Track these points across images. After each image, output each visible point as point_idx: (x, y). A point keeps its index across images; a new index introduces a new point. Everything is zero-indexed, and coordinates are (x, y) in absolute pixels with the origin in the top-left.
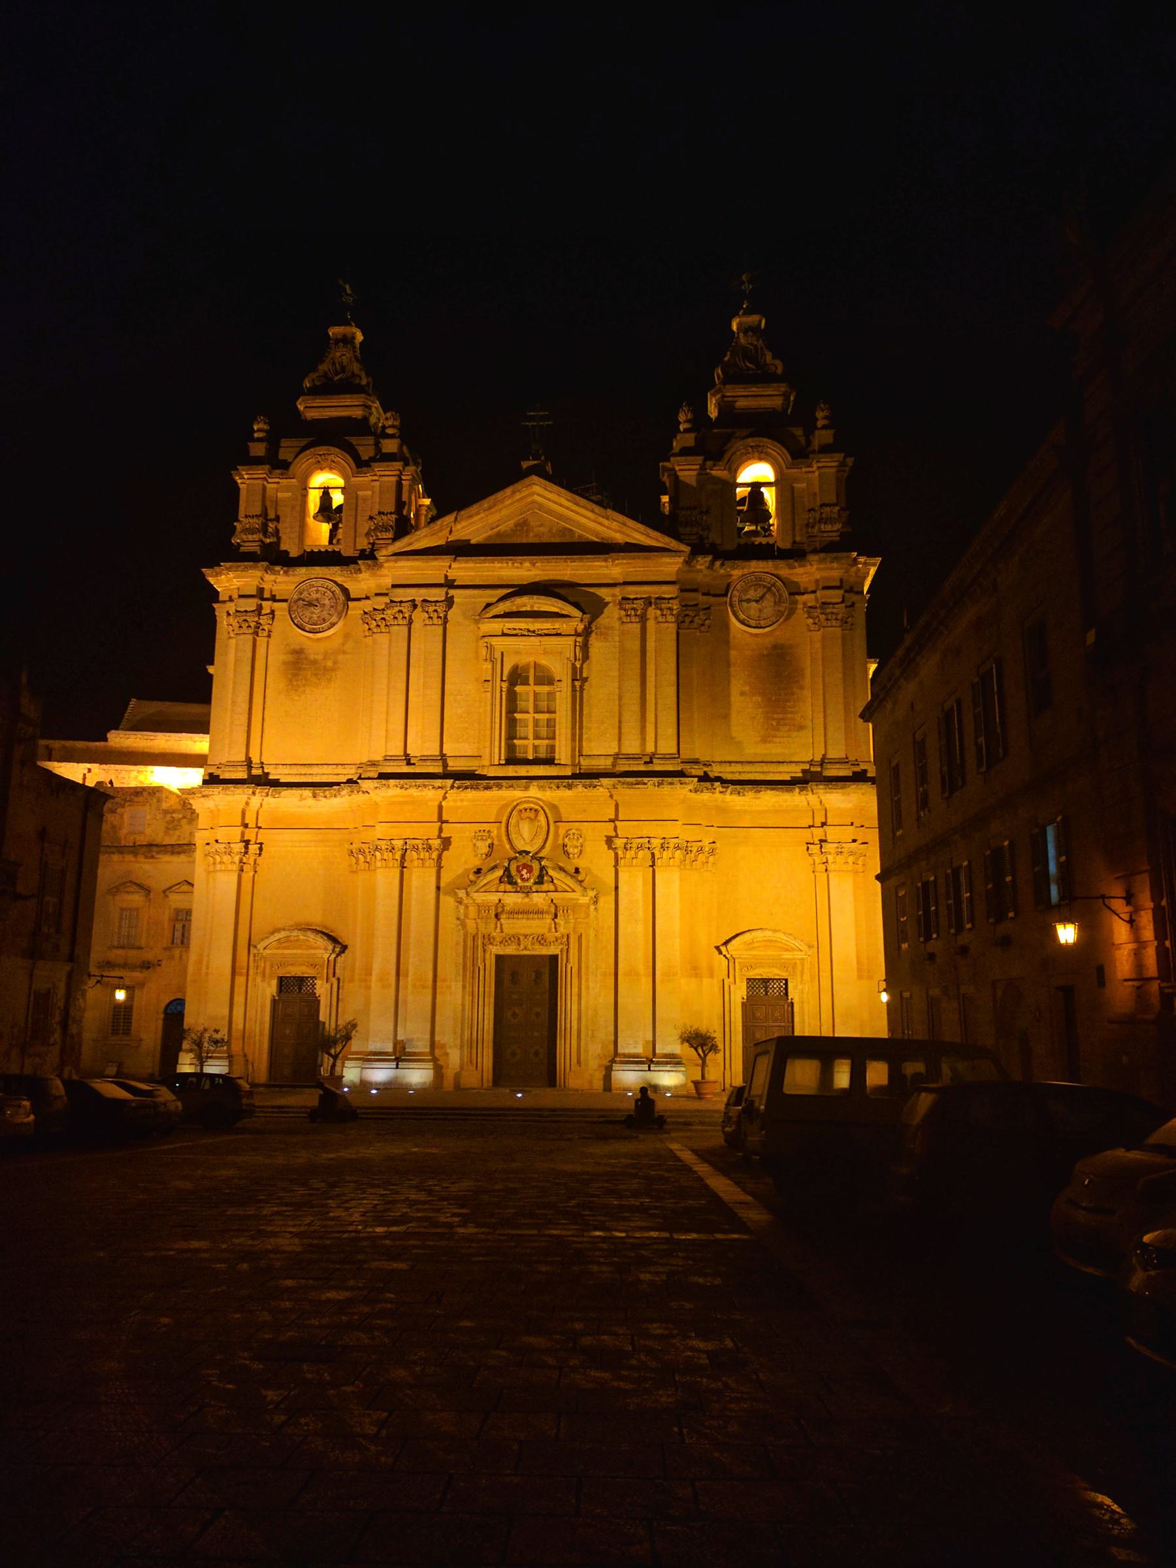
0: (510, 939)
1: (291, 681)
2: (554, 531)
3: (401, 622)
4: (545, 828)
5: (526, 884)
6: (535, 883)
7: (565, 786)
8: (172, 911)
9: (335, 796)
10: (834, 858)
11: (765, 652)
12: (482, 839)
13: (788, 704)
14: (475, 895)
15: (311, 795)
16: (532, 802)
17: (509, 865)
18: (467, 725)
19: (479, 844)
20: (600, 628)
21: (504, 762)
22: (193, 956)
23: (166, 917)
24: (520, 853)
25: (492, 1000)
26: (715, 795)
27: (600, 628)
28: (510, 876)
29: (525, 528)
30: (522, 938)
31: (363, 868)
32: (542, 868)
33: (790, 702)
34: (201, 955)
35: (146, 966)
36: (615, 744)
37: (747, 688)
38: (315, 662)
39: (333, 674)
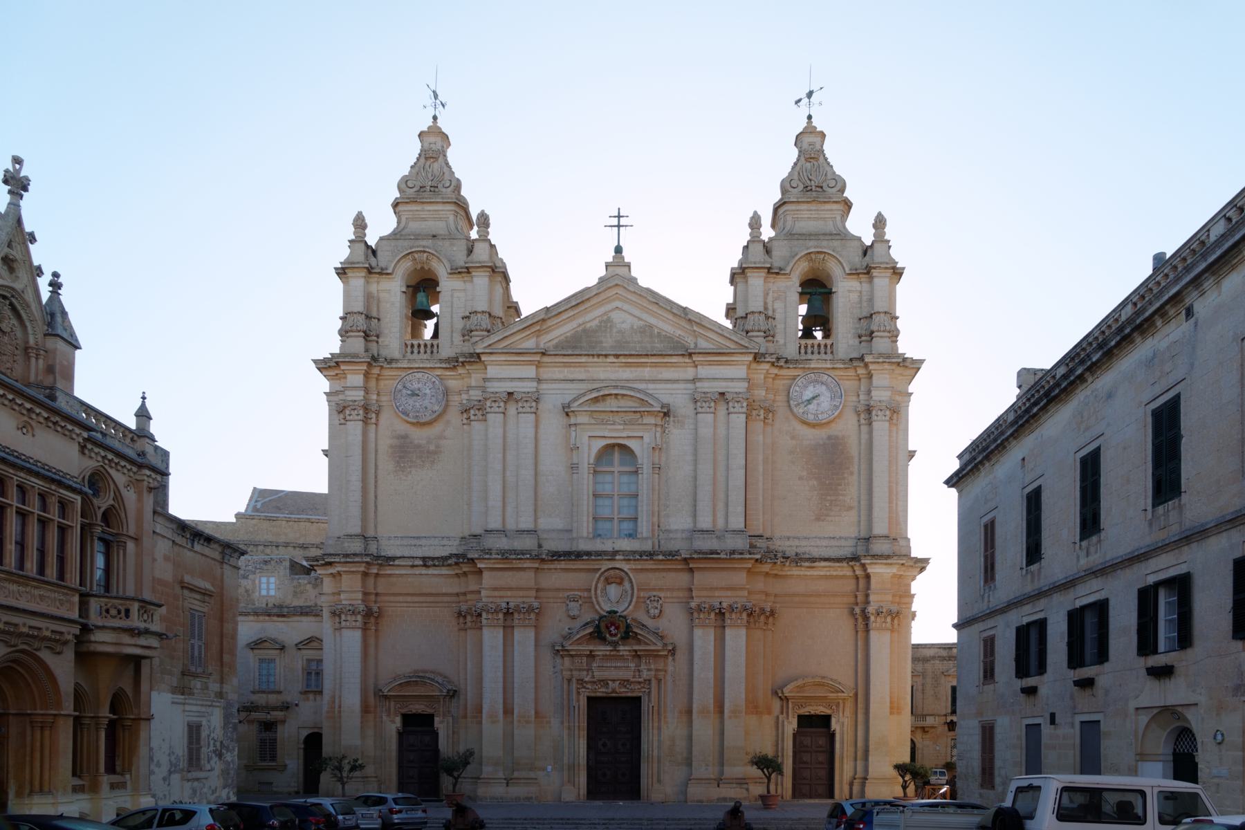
1: (398, 462)
4: (630, 592)
5: (614, 639)
6: (622, 638)
8: (305, 661)
12: (574, 601)
15: (421, 563)
19: (572, 604)
21: (591, 536)
23: (300, 667)
24: (609, 612)
25: (586, 732)
30: (609, 682)
35: (286, 707)
36: (689, 520)
38: (419, 446)
39: (436, 457)
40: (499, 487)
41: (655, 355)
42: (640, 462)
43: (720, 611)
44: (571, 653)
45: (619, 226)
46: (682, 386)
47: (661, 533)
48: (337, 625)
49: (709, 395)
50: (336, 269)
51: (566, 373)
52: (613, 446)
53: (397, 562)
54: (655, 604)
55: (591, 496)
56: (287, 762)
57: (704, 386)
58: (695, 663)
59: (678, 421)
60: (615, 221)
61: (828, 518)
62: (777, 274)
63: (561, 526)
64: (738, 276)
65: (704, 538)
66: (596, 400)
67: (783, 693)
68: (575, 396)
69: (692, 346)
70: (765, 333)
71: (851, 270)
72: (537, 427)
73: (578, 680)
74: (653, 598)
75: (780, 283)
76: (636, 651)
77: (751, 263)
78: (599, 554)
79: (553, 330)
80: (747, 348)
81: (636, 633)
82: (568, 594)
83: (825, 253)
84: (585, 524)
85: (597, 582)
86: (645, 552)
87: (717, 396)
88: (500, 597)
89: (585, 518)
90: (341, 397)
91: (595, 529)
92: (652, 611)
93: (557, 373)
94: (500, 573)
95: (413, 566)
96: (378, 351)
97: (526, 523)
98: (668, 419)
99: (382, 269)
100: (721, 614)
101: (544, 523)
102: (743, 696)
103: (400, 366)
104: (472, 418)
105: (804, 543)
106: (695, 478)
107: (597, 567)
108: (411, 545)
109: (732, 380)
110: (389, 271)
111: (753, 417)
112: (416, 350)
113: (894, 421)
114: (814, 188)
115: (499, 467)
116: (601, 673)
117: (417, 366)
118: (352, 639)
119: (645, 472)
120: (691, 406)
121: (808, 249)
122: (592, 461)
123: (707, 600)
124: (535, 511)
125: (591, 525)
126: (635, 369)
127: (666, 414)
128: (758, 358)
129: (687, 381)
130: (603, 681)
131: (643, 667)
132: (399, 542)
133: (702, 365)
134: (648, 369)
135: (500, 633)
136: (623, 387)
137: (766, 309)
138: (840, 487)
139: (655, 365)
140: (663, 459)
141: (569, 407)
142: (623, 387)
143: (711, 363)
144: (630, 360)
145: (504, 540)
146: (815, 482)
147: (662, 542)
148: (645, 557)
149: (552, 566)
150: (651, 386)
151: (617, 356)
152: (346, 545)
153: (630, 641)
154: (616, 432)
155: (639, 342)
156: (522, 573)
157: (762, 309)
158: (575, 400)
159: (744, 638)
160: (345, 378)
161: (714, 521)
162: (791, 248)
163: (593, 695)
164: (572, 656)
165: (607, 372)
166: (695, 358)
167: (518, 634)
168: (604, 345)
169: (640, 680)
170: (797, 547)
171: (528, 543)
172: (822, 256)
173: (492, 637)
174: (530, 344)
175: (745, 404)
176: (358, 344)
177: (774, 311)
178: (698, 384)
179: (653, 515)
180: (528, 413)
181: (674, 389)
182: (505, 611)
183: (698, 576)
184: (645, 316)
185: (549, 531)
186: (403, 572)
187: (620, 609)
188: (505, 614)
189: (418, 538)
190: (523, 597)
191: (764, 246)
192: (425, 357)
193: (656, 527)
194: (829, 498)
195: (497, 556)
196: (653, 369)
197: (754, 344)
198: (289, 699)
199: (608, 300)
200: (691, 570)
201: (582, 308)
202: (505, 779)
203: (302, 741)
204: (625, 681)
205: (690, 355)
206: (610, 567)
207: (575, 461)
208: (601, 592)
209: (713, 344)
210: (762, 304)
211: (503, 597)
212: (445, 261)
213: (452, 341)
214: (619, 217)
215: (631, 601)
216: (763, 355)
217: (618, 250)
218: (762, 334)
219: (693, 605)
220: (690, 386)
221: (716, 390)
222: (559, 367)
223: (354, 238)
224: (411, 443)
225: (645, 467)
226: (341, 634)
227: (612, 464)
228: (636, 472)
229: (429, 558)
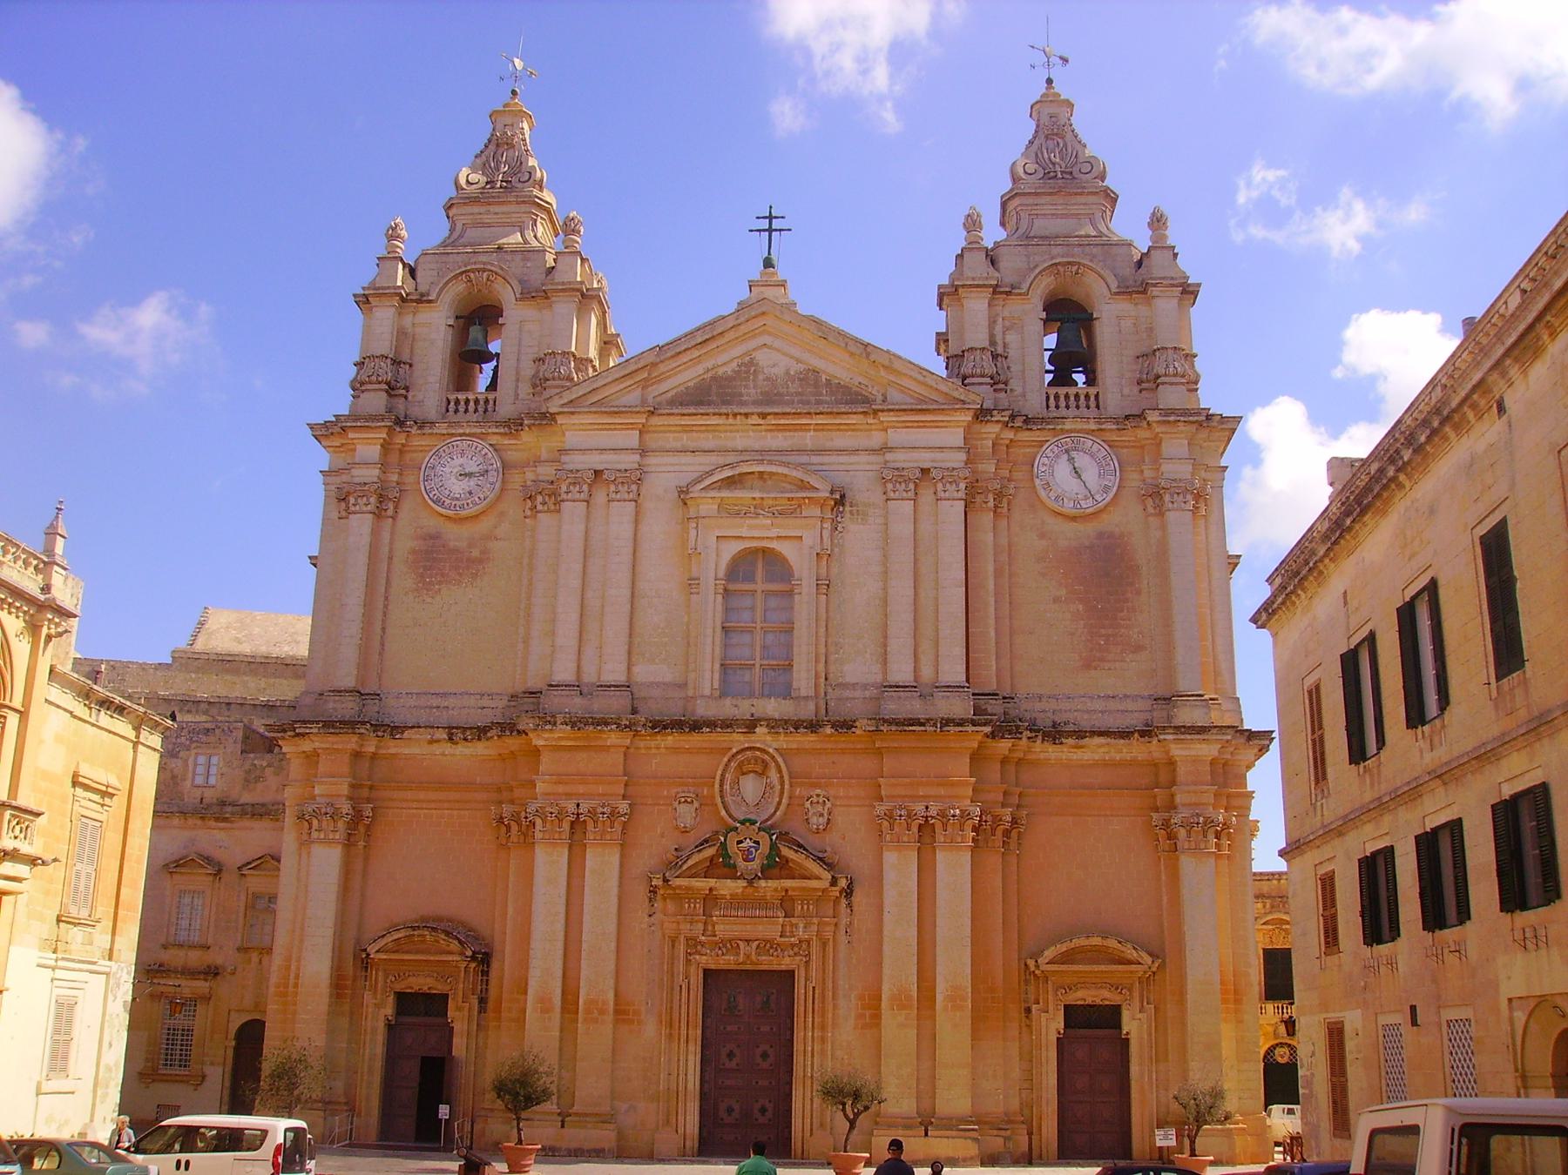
0: (725, 946)
2: (792, 373)
3: (578, 496)
7: (806, 728)
8: (250, 897)
9: (479, 739)
10: (1189, 832)
11: (1087, 544)
13: (1122, 614)
14: (678, 882)
15: (445, 736)
16: (759, 749)
17: (725, 840)
20: (857, 505)
21: (717, 693)
22: (277, 960)
26: (1021, 743)
27: (857, 505)
28: (727, 856)
29: (753, 369)
31: (516, 840)
32: (773, 846)
33: (1122, 611)
34: (288, 959)
36: (877, 668)
37: (1063, 592)
40: (575, 616)
41: (822, 413)
42: (796, 576)
45: (770, 230)
46: (863, 458)
47: (830, 690)
48: (305, 837)
49: (904, 473)
50: (355, 296)
51: (686, 440)
52: (753, 552)
53: (406, 735)
54: (820, 808)
55: (719, 629)
56: (208, 1070)
57: (899, 458)
58: (886, 909)
60: (765, 224)
62: (1008, 293)
63: (669, 678)
64: (948, 296)
65: (900, 698)
66: (730, 482)
67: (1037, 967)
68: (696, 475)
69: (880, 398)
70: (992, 379)
71: (1118, 287)
72: (637, 522)
74: (815, 799)
75: (1013, 307)
77: (967, 279)
78: (728, 724)
79: (669, 377)
80: (963, 402)
83: (1079, 263)
84: (708, 675)
85: (724, 771)
86: (803, 721)
87: (918, 474)
89: (708, 666)
90: (345, 478)
91: (724, 681)
92: (814, 820)
93: (672, 440)
95: (431, 742)
96: (407, 409)
97: (614, 672)
99: (422, 295)
100: (926, 828)
101: (642, 673)
102: (968, 971)
106: (885, 602)
107: (724, 745)
108: (431, 707)
110: (430, 298)
111: (977, 505)
112: (462, 408)
115: (576, 583)
118: (327, 860)
119: (805, 590)
120: (880, 490)
121: (1052, 258)
122: (721, 574)
124: (629, 653)
125: (717, 676)
126: (792, 434)
127: (841, 501)
128: (982, 415)
129: (874, 451)
132: (412, 702)
133: (892, 427)
134: (812, 433)
135: (563, 855)
137: (993, 343)
139: (819, 428)
140: (834, 570)
141: (687, 492)
142: (771, 462)
143: (907, 425)
144: (782, 422)
145: (578, 700)
148: (802, 730)
149: (653, 744)
150: (815, 459)
151: (763, 416)
152: (331, 705)
153: (776, 871)
154: (760, 531)
155: (798, 394)
157: (986, 344)
160: (355, 450)
161: (916, 670)
162: (1028, 256)
165: (746, 436)
166: (884, 417)
167: (592, 859)
171: (615, 704)
172: (1076, 268)
173: (549, 863)
174: (633, 397)
175: (962, 486)
176: (376, 401)
177: (1005, 345)
178: (889, 456)
179: (817, 661)
180: (625, 501)
181: (851, 464)
183: (889, 764)
184: (806, 356)
185: (651, 685)
186: (416, 750)
188: (572, 823)
189: (444, 695)
191: (987, 256)
192: (475, 417)
193: (823, 680)
196: (820, 434)
197: (972, 397)
198: (219, 961)
199: (752, 334)
200: (879, 753)
201: (713, 345)
202: (559, 1114)
203: (232, 1034)
205: (875, 412)
207: (694, 575)
208: (731, 788)
209: (912, 397)
212: (515, 283)
213: (517, 395)
214: (770, 218)
215: (779, 803)
216: (989, 412)
217: (768, 263)
219: (881, 809)
220: (879, 459)
221: (916, 465)
222: (675, 432)
223: (384, 253)
225: (804, 583)
226: (309, 853)
227: (752, 580)
228: (790, 594)
229: (457, 728)
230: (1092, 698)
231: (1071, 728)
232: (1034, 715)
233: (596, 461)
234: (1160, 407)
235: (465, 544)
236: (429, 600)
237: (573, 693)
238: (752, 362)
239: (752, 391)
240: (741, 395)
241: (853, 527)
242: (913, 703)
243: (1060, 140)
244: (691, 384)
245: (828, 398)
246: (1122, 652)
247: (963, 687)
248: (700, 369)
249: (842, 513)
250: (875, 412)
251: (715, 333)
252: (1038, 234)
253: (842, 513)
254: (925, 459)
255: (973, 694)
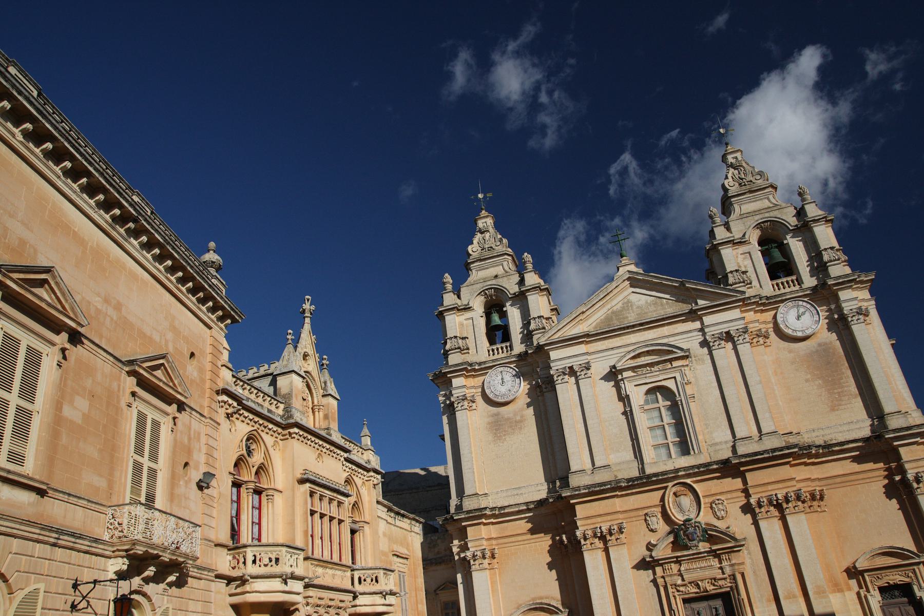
2: (649, 302)
18: (622, 439)
20: (697, 356)
29: (630, 304)
30: (699, 582)
36: (729, 432)
43: (777, 502)
44: (660, 562)
54: (720, 506)
59: (699, 359)
61: (840, 407)
65: (745, 444)
66: (634, 358)
70: (744, 282)
73: (671, 585)
74: (717, 502)
76: (715, 551)
78: (663, 473)
81: (711, 536)
82: (646, 511)
83: (770, 221)
88: (593, 524)
94: (588, 504)
98: (690, 359)
102: (822, 576)
103: (487, 365)
104: (544, 390)
105: (827, 431)
109: (732, 321)
113: (868, 321)
114: (746, 183)
116: (690, 576)
117: (499, 363)
123: (764, 495)
130: (693, 582)
131: (725, 564)
136: (652, 345)
137: (740, 267)
138: (842, 381)
142: (652, 345)
145: (587, 477)
146: (820, 382)
147: (712, 454)
150: (671, 339)
155: (655, 311)
156: (606, 501)
158: (619, 361)
159: (805, 523)
162: (744, 223)
163: (686, 596)
164: (661, 565)
168: (630, 318)
169: (725, 576)
170: (823, 436)
182: (599, 535)
187: (693, 516)
190: (611, 520)
194: (836, 391)
195: (585, 491)
201: (608, 298)
204: (711, 579)
206: (676, 482)
210: (736, 264)
211: (595, 523)
216: (749, 298)
218: (743, 284)
224: (502, 418)
230: (840, 425)
231: (834, 442)
232: (814, 439)
233: (567, 363)
234: (832, 277)
235: (512, 415)
236: (502, 444)
237: (584, 474)
238: (629, 302)
239: (633, 314)
240: (627, 317)
241: (698, 367)
242: (753, 445)
243: (741, 168)
244: (602, 317)
245: (669, 310)
246: (848, 399)
247: (776, 432)
248: (605, 310)
249: (691, 361)
250: (695, 311)
251: (608, 292)
252: (745, 212)
253: (691, 361)
254: (724, 328)
255: (782, 435)
